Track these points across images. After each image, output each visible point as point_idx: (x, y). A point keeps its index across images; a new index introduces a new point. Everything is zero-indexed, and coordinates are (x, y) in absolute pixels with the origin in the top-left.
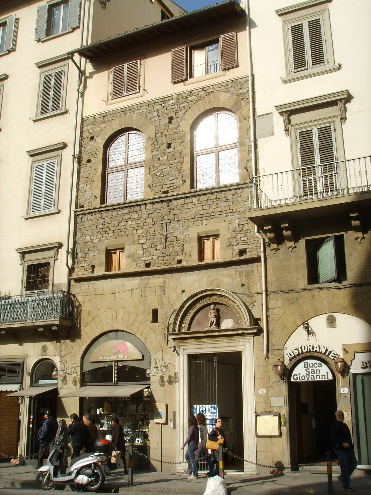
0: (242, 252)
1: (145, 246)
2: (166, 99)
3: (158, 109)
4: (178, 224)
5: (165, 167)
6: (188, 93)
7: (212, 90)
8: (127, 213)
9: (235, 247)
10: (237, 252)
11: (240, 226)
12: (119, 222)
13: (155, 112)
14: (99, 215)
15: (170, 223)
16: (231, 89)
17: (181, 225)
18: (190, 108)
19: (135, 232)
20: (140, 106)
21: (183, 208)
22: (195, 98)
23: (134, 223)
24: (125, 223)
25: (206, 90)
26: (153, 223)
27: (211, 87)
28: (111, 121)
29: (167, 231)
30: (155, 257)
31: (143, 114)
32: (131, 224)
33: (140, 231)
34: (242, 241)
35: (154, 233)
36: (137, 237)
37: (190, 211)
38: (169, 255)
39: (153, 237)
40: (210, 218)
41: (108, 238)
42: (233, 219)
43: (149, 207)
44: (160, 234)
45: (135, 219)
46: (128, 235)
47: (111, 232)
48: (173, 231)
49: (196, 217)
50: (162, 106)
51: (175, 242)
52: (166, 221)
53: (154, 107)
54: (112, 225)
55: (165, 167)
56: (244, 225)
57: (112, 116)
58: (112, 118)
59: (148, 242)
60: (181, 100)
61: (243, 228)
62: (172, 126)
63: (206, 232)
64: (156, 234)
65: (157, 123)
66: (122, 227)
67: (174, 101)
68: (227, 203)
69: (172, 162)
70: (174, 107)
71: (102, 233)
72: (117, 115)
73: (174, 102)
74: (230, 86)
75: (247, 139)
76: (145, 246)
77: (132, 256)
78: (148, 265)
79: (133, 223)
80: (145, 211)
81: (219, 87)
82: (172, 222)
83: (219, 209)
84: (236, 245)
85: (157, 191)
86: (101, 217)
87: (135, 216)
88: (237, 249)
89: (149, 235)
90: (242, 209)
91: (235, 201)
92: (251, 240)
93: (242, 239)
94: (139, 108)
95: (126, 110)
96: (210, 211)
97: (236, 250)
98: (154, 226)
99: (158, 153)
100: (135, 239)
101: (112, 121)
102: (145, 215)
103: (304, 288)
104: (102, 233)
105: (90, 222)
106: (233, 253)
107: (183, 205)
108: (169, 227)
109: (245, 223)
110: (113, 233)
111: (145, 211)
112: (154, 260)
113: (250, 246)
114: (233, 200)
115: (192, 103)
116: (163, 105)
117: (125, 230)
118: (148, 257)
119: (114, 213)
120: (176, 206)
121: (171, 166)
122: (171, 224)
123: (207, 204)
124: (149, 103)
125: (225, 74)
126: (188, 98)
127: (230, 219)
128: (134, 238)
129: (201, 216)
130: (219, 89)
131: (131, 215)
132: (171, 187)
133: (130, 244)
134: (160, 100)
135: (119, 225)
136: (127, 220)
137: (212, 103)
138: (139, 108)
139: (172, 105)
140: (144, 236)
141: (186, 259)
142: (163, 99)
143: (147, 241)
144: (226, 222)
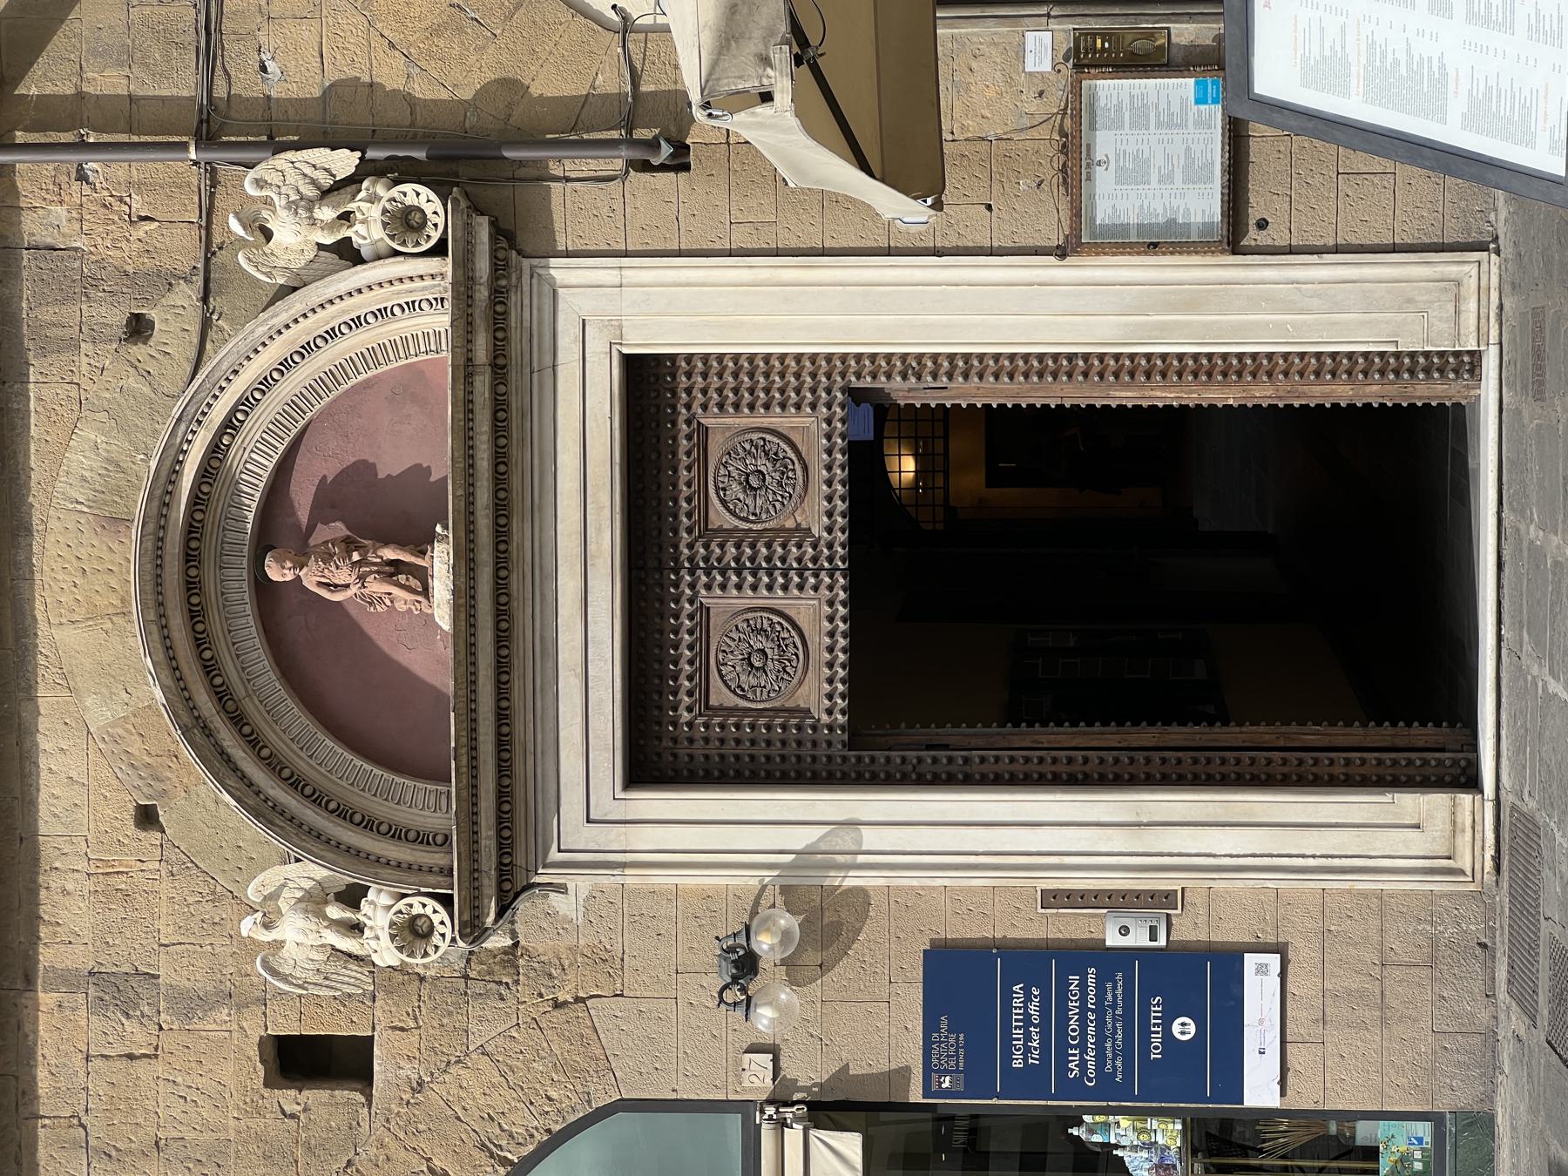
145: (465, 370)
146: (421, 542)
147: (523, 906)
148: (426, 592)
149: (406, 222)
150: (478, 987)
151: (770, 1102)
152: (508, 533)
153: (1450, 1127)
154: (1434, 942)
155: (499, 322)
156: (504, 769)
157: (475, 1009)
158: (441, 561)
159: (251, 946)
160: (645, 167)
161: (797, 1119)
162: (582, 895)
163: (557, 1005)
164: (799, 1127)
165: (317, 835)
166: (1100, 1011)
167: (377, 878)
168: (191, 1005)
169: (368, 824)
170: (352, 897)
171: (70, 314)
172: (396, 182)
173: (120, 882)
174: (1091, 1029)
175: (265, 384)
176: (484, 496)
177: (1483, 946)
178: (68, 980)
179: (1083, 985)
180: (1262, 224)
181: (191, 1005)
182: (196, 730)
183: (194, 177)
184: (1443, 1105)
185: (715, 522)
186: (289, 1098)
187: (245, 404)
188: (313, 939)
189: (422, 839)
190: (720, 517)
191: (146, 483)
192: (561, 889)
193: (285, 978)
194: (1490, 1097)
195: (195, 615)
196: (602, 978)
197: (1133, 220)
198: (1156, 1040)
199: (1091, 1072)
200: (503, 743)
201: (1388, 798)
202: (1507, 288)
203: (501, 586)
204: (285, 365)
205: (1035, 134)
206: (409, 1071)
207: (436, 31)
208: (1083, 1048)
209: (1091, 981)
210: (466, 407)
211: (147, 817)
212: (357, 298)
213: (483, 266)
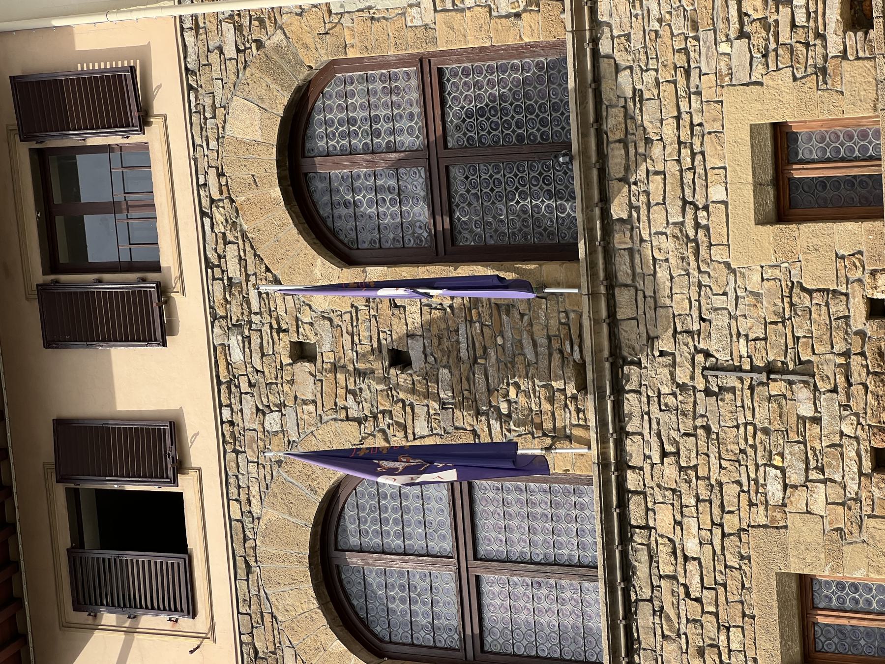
1: (795, 476)
2: (224, 376)
3: (258, 409)
4: (713, 316)
5: (479, 377)
6: (214, 279)
7: (212, 172)
8: (651, 558)
9: (834, 49)
10: (854, 39)
11: (747, 29)
12: (682, 596)
13: (267, 426)
15: (707, 354)
16: (219, 94)
17: (719, 302)
18: (268, 270)
19: (731, 523)
20: (233, 490)
21: (649, 293)
22: (235, 247)
23: (693, 523)
24: (692, 566)
25: (212, 201)
26: (700, 432)
27: (201, 181)
28: (275, 625)
29: (739, 369)
30: (848, 430)
31: (268, 477)
32: (697, 541)
33: (731, 490)
34: (808, 21)
35: (742, 429)
36: (754, 509)
37: (667, 260)
38: (842, 360)
39: (759, 435)
40: (700, 170)
42: (713, 63)
43: (632, 447)
44: (748, 403)
46: (742, 558)
47: (723, 637)
48: (742, 341)
49: (691, 234)
50: (247, 393)
52: (698, 372)
54: (691, 630)
55: (479, 377)
56: (746, 14)
57: (256, 617)
58: (267, 618)
59: (777, 461)
60: (235, 311)
61: (755, 16)
62: (326, 347)
63: (758, 186)
64: (750, 419)
67: (234, 341)
68: (646, 95)
69: (463, 346)
72: (258, 596)
73: (240, 338)
74: (208, 101)
75: (408, 19)
76: (795, 476)
77: (836, 536)
79: (695, 530)
80: (647, 468)
81: (204, 144)
82: (702, 346)
83: (669, 131)
84: (825, 47)
85: (574, 414)
87: (664, 519)
88: (839, 40)
89: (750, 451)
90: (679, 25)
91: (643, 57)
93: (800, 19)
94: (243, 497)
95: (242, 552)
96: (672, 168)
97: (844, 44)
98: (714, 428)
99: (421, 411)
100: (762, 520)
101: (280, 618)
102: (667, 472)
106: (858, 58)
107: (640, 294)
108: (723, 357)
110: (728, 629)
111: (647, 468)
112: (859, 432)
114: (636, 70)
115: (250, 259)
116: (245, 387)
117: (720, 567)
119: (644, 618)
120: (642, 328)
121: (479, 352)
122: (712, 351)
123: (642, 188)
124: (229, 448)
126: (230, 279)
127: (713, 77)
128: (759, 526)
129: (690, 211)
130: (213, 144)
131: (660, 540)
132: (561, 352)
134: (225, 401)
135: (698, 600)
136: (680, 560)
137: (259, 172)
138: (243, 497)
139: (250, 348)
140: (753, 476)
141: (867, 279)
142: (223, 387)
143: (775, 463)
144: (726, 95)
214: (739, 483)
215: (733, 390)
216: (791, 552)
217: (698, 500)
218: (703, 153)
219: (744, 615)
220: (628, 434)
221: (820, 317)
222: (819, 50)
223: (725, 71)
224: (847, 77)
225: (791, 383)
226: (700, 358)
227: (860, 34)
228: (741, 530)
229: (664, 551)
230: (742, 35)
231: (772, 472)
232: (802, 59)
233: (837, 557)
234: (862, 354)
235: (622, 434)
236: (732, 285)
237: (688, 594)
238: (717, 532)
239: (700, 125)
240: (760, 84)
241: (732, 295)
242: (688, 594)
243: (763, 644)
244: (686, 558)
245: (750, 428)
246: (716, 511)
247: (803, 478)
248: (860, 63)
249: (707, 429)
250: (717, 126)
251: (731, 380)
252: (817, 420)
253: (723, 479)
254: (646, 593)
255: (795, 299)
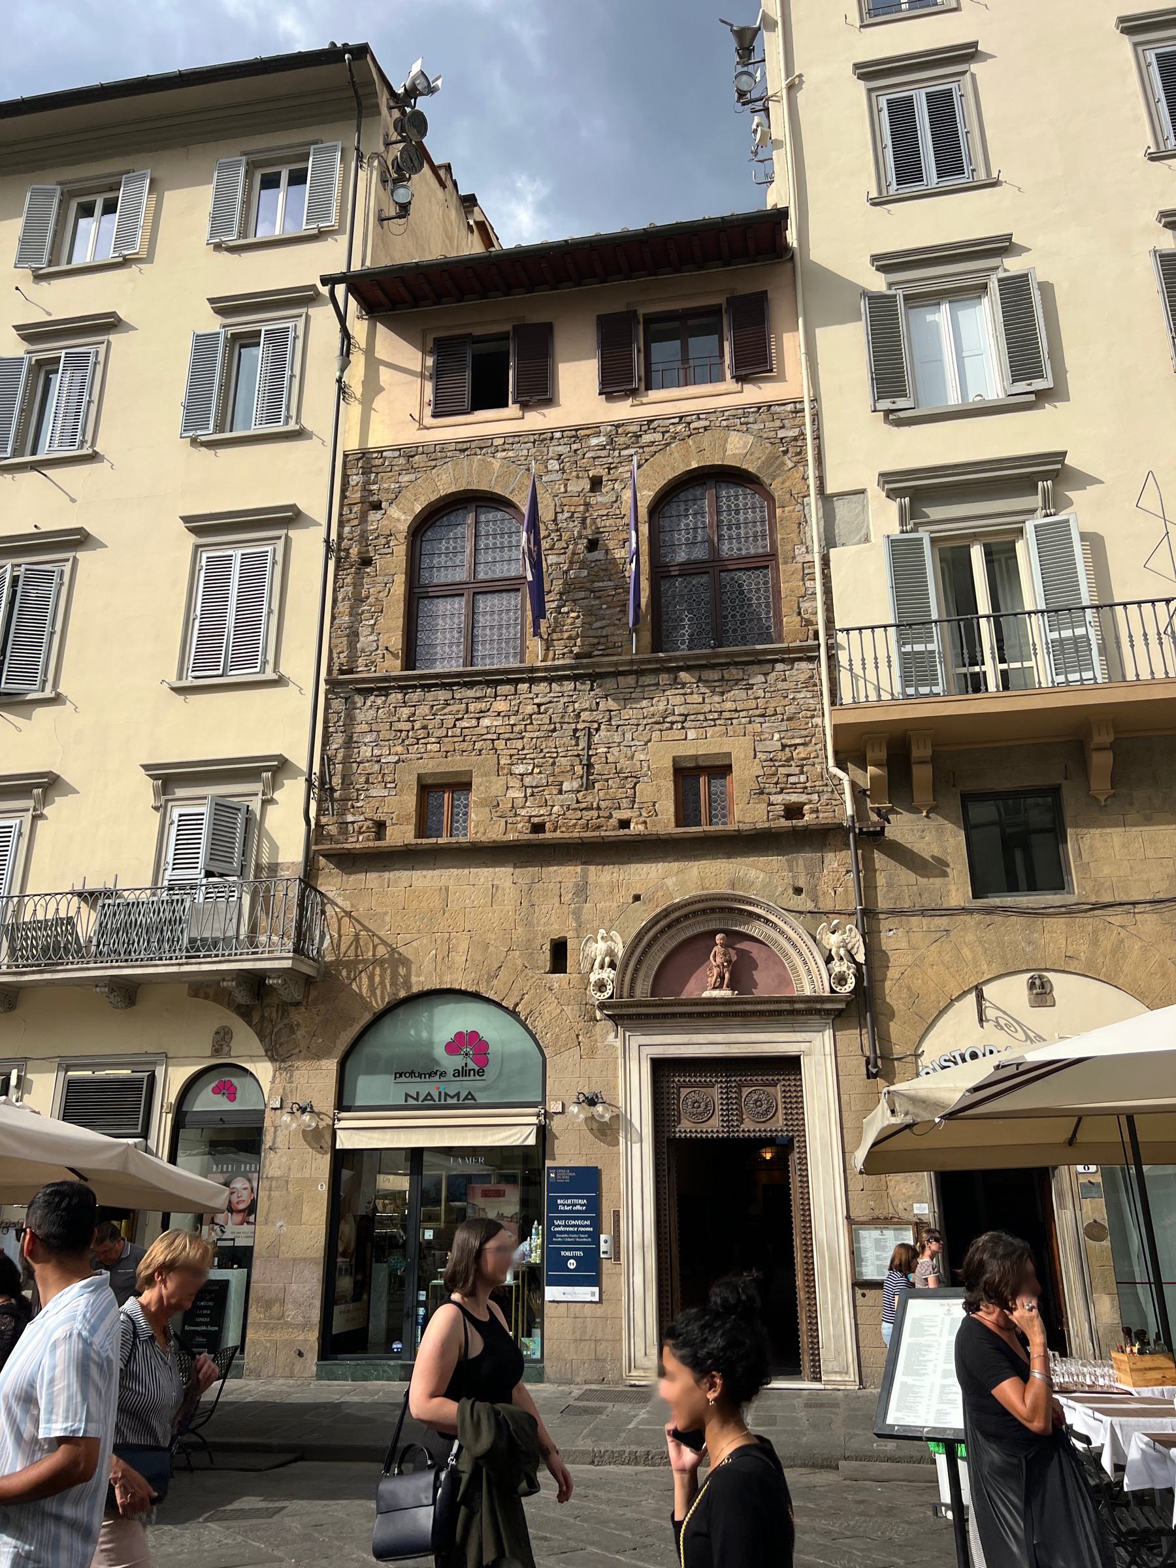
0: (793, 811)
1: (528, 780)
3: (561, 455)
5: (582, 594)
6: (641, 425)
7: (707, 423)
8: (478, 698)
9: (774, 799)
11: (787, 749)
12: (457, 717)
13: (551, 461)
14: (400, 696)
15: (598, 730)
16: (755, 427)
17: (628, 736)
18: (647, 460)
19: (500, 744)
20: (511, 440)
21: (633, 695)
24: (474, 722)
25: (689, 424)
26: (553, 726)
27: (701, 416)
29: (589, 748)
30: (555, 809)
32: (489, 724)
33: (519, 744)
34: (791, 784)
35: (554, 750)
38: (595, 805)
39: (551, 760)
40: (705, 724)
41: (425, 756)
43: (543, 687)
44: (570, 753)
45: (502, 714)
46: (480, 751)
47: (433, 740)
49: (668, 720)
51: (611, 776)
52: (587, 725)
53: (551, 449)
54: (437, 722)
55: (582, 594)
58: (433, 463)
59: (536, 770)
60: (621, 440)
62: (599, 499)
63: (696, 757)
65: (559, 489)
66: (466, 732)
67: (602, 440)
68: (750, 692)
69: (601, 584)
70: (603, 453)
71: (407, 742)
72: (446, 457)
74: (751, 420)
76: (528, 780)
77: (495, 803)
78: (538, 828)
79: (495, 723)
80: (531, 696)
82: (603, 727)
83: (729, 705)
84: (775, 794)
85: (562, 652)
86: (404, 702)
87: (501, 706)
88: (779, 802)
89: (542, 755)
90: (790, 710)
91: (772, 689)
92: (817, 783)
93: (792, 779)
94: (507, 446)
95: (473, 446)
96: (707, 708)
98: (554, 734)
99: (562, 559)
100: (502, 762)
101: (434, 471)
102: (529, 707)
103: (963, 905)
104: (407, 742)
105: (372, 712)
106: (768, 812)
107: (632, 690)
108: (596, 739)
109: (798, 741)
110: (439, 743)
111: (531, 696)
112: (554, 816)
113: (815, 797)
114: (765, 686)
115: (653, 449)
116: (575, 447)
118: (537, 809)
119: (443, 695)
120: (613, 691)
121: (597, 594)
123: (695, 690)
124: (536, 437)
125: (739, 389)
126: (641, 436)
129: (681, 718)
130: (724, 423)
132: (598, 643)
133: (485, 775)
134: (565, 434)
135: (455, 726)
136: (477, 715)
137: (707, 454)
138: (507, 446)
141: (641, 819)
142: (574, 433)
145: (791, 1000)
146: (731, 987)
147: (610, 1023)
148: (714, 988)
149: (842, 979)
150: (583, 1009)
151: (546, 1111)
152: (736, 1016)
153: (539, 1365)
154: (604, 1360)
155: (809, 1012)
156: (656, 1016)
157: (576, 1007)
158: (725, 993)
159: (596, 933)
160: (868, 1063)
161: (540, 1121)
162: (614, 1044)
163: (578, 1036)
164: (537, 1122)
165: (632, 953)
166: (578, 1232)
167: (618, 974)
168: (577, 914)
169: (636, 970)
170: (612, 965)
171: (801, 869)
172: (855, 976)
173: (616, 891)
174: (571, 1229)
175: (782, 933)
176: (748, 1008)
177: (603, 1380)
178: (585, 875)
179: (586, 1226)
180: (864, 1295)
181: (577, 914)
182: (666, 913)
183: (851, 908)
184: (546, 1363)
185: (744, 1089)
186: (547, 947)
187: (775, 926)
188: (598, 952)
189: (632, 988)
190: (746, 1091)
191: (746, 895)
192: (616, 1037)
193: (586, 944)
194: (549, 1382)
195: (704, 911)
196: (586, 1051)
197: (862, 1245)
198: (568, 1254)
199: (556, 1229)
200: (665, 1016)
201: (656, 1343)
202: (846, 1393)
203: (717, 1014)
204: (789, 939)
205: (891, 1207)
206: (556, 985)
207: (909, 988)
208: (565, 1226)
209: (588, 1229)
210: (778, 1001)
211: (637, 898)
212: (813, 963)
213: (828, 1006)
214: (523, 749)
215: (577, 745)
216: (484, 779)
217: (513, 725)
218: (715, 725)
219: (447, 752)
220: (550, 684)
221: (620, 793)
222: (774, 790)
223: (762, 737)
224: (758, 806)
225: (582, 777)
226: (595, 725)
227: (782, 813)
228: (496, 750)
229: (483, 706)
230: (784, 747)
231: (530, 768)
232: (768, 781)
233: (483, 803)
234: (599, 817)
235: (550, 680)
236: (638, 743)
237: (458, 720)
238: (495, 736)
239: (732, 724)
240: (755, 758)
241: (632, 743)
242: (458, 720)
243: (432, 763)
244: (478, 719)
245: (555, 755)
246: (507, 736)
247: (527, 785)
248: (766, 813)
249: (554, 730)
250: (730, 733)
251: (583, 744)
252: (560, 792)
253: (525, 740)
254: (457, 696)
255: (630, 779)
